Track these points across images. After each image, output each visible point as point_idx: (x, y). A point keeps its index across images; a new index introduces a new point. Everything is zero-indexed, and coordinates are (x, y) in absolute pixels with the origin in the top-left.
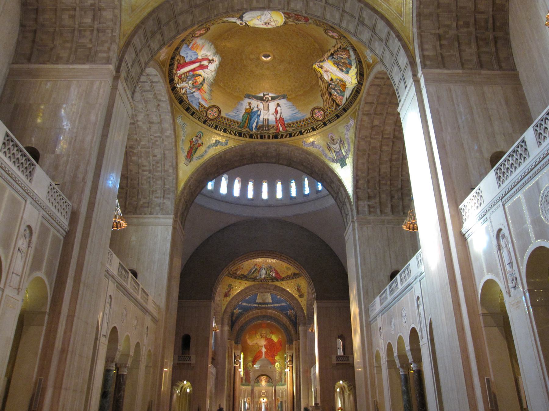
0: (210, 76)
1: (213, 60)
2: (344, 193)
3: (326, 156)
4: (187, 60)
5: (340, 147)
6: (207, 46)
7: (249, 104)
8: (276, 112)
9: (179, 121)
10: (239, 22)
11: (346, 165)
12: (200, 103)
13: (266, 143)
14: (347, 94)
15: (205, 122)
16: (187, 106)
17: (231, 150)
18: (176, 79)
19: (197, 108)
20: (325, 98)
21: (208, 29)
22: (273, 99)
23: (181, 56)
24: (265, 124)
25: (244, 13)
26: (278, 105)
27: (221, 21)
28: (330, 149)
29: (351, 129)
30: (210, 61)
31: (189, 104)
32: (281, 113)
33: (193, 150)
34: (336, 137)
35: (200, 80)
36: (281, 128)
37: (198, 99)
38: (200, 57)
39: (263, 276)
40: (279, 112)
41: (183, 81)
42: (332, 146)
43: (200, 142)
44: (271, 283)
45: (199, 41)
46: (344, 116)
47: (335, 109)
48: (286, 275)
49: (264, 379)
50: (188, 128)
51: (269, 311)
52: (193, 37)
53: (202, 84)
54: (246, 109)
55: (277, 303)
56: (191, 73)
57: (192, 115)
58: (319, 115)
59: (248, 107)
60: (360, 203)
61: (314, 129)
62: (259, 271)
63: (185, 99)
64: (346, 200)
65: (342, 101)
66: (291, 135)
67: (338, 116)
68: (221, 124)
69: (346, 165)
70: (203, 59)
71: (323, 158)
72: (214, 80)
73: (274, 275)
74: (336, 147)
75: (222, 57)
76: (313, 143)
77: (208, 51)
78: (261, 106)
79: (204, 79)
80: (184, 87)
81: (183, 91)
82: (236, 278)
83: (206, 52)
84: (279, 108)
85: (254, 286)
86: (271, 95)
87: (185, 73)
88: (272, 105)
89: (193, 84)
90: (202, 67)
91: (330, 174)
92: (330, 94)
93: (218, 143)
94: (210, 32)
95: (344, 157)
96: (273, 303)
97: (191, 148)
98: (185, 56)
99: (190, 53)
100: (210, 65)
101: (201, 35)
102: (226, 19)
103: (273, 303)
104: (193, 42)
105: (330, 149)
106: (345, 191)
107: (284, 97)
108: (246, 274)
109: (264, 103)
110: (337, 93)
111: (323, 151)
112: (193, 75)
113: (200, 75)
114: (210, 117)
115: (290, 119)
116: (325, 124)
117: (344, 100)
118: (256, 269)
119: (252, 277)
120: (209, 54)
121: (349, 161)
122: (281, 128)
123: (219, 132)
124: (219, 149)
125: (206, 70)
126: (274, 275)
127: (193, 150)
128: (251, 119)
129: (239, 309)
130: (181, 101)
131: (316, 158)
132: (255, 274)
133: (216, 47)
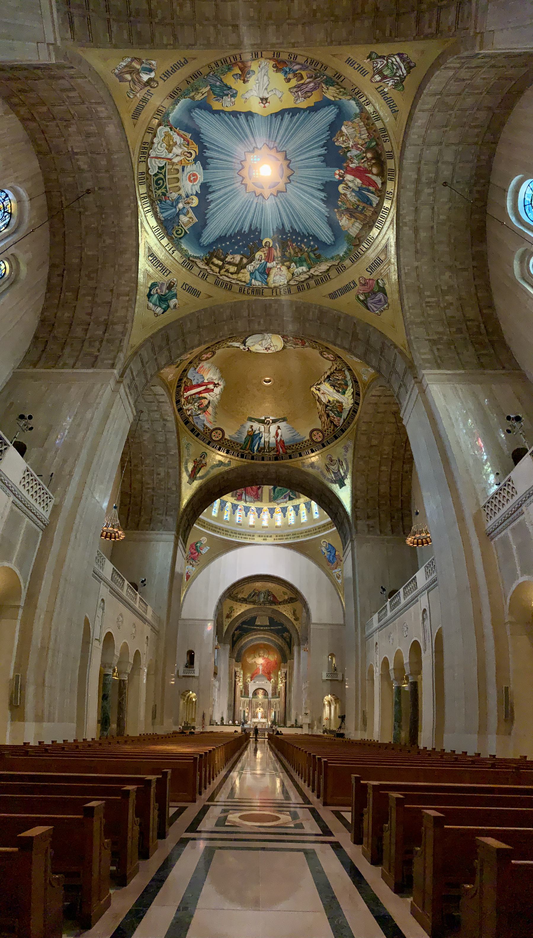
0: (215, 399)
1: (218, 384)
2: (342, 512)
3: (325, 476)
4: (194, 383)
5: (339, 467)
6: (213, 370)
7: (252, 426)
8: (277, 434)
9: (184, 441)
10: (242, 347)
11: (345, 485)
12: (204, 425)
13: (267, 465)
14: (344, 415)
15: (209, 444)
16: (192, 427)
17: (232, 470)
18: (183, 400)
19: (202, 429)
20: (323, 420)
21: (214, 353)
22: (274, 421)
23: (188, 378)
24: (267, 445)
25: (247, 338)
26: (279, 428)
27: (226, 346)
28: (328, 470)
29: (349, 449)
30: (216, 385)
31: (194, 425)
32: (281, 436)
33: (197, 470)
34: (335, 458)
35: (205, 402)
36: (281, 450)
37: (204, 421)
38: (206, 381)
40: (280, 434)
41: (189, 403)
42: (331, 467)
43: (204, 462)
45: (205, 365)
46: (342, 437)
47: (333, 430)
50: (193, 447)
52: (201, 360)
53: (207, 406)
54: (248, 432)
56: (197, 396)
57: (197, 436)
58: (318, 437)
59: (250, 430)
60: (359, 522)
61: (313, 451)
63: (191, 419)
64: (345, 521)
65: (340, 422)
66: (290, 457)
67: (336, 438)
68: (224, 444)
69: (345, 485)
70: (209, 383)
71: (321, 478)
72: (218, 402)
74: (334, 468)
75: (226, 381)
76: (312, 465)
77: (214, 375)
78: (262, 429)
79: (209, 402)
80: (190, 408)
81: (189, 413)
83: (211, 376)
84: (279, 431)
86: (272, 418)
87: (191, 395)
88: (273, 428)
89: (198, 406)
90: (207, 390)
91: (328, 494)
92: (328, 416)
93: (221, 463)
94: (215, 356)
95: (342, 477)
97: (194, 468)
98: (192, 379)
99: (197, 376)
100: (215, 389)
101: (207, 359)
102: (231, 344)
104: (200, 365)
105: (328, 470)
106: (344, 510)
107: (284, 420)
109: (265, 426)
110: (335, 414)
111: (321, 472)
112: (199, 398)
113: (205, 398)
114: (214, 438)
115: (290, 442)
116: (324, 446)
117: (342, 421)
120: (214, 378)
121: (348, 481)
122: (281, 450)
123: (222, 453)
124: (223, 469)
125: (211, 393)
127: (197, 470)
128: (252, 441)
130: (187, 422)
131: (315, 478)
133: (221, 371)
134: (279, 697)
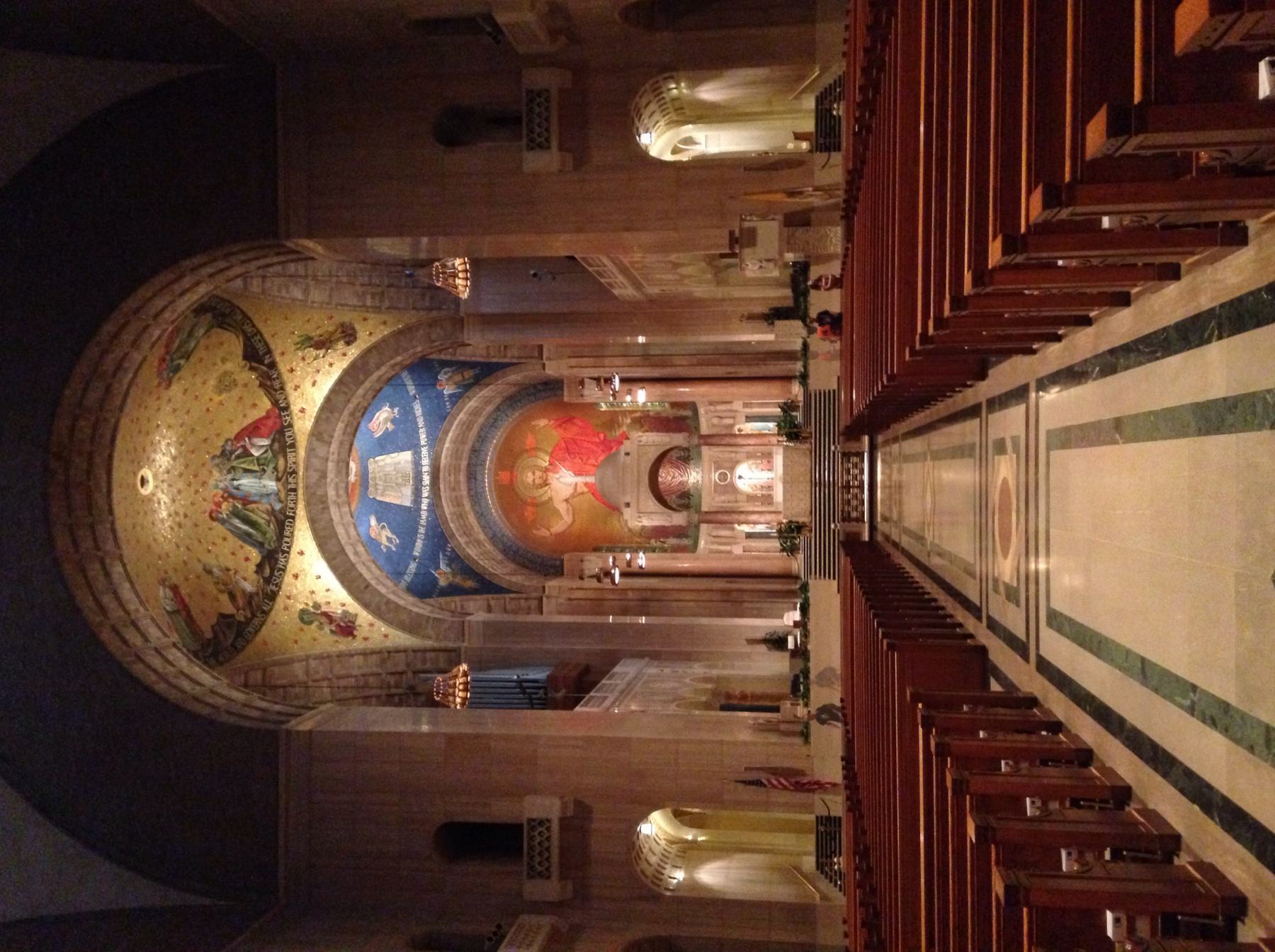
39: (271, 485)
44: (302, 452)
48: (262, 392)
49: (668, 476)
51: (443, 461)
55: (416, 430)
62: (246, 501)
73: (266, 442)
82: (273, 597)
85: (313, 522)
96: (415, 447)
103: (415, 447)
108: (255, 555)
118: (235, 513)
119: (271, 530)
126: (266, 442)
129: (438, 568)
132: (261, 519)
134: (693, 407)
